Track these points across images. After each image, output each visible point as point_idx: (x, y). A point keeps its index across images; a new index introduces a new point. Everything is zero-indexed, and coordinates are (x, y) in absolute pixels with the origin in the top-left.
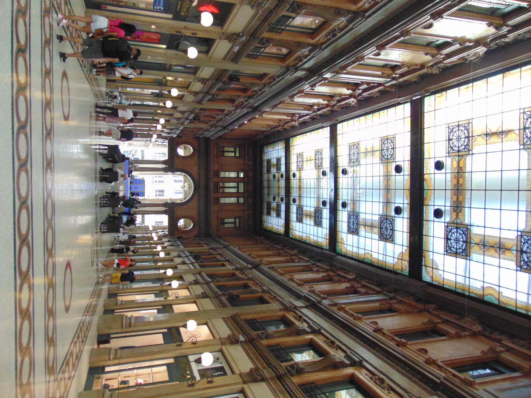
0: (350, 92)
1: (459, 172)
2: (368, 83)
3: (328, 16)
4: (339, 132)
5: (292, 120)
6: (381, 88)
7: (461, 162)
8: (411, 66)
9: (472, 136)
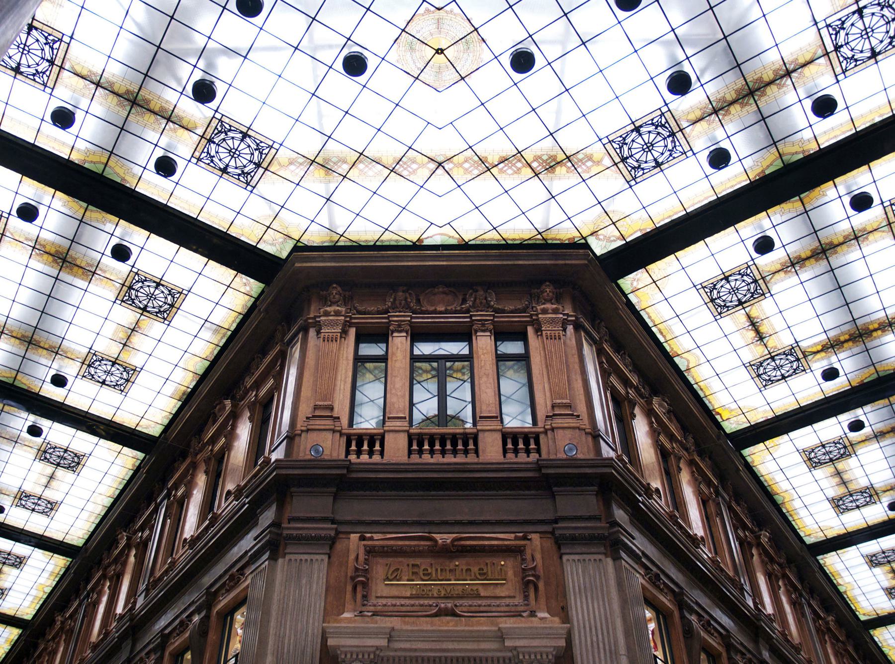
0: (754, 551)
1: (832, 346)
2: (735, 528)
3: (696, 646)
4: (820, 537)
5: (829, 629)
6: (734, 504)
7: (814, 350)
8: (696, 480)
9: (770, 353)
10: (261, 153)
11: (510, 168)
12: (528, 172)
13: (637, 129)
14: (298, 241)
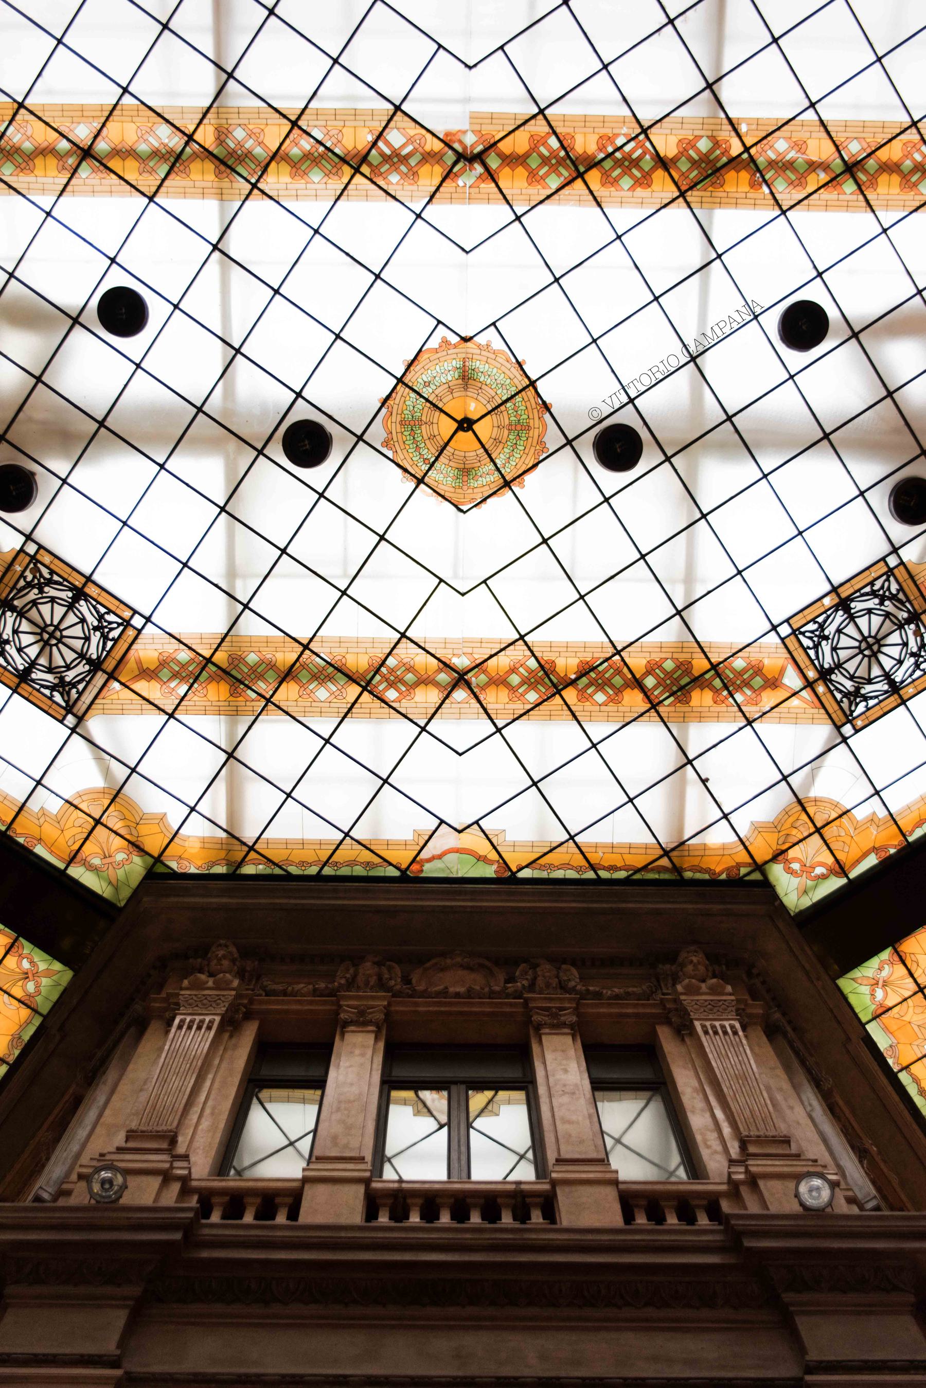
10: (105, 637)
11: (600, 688)
12: (634, 700)
13: (844, 605)
14: (158, 860)
